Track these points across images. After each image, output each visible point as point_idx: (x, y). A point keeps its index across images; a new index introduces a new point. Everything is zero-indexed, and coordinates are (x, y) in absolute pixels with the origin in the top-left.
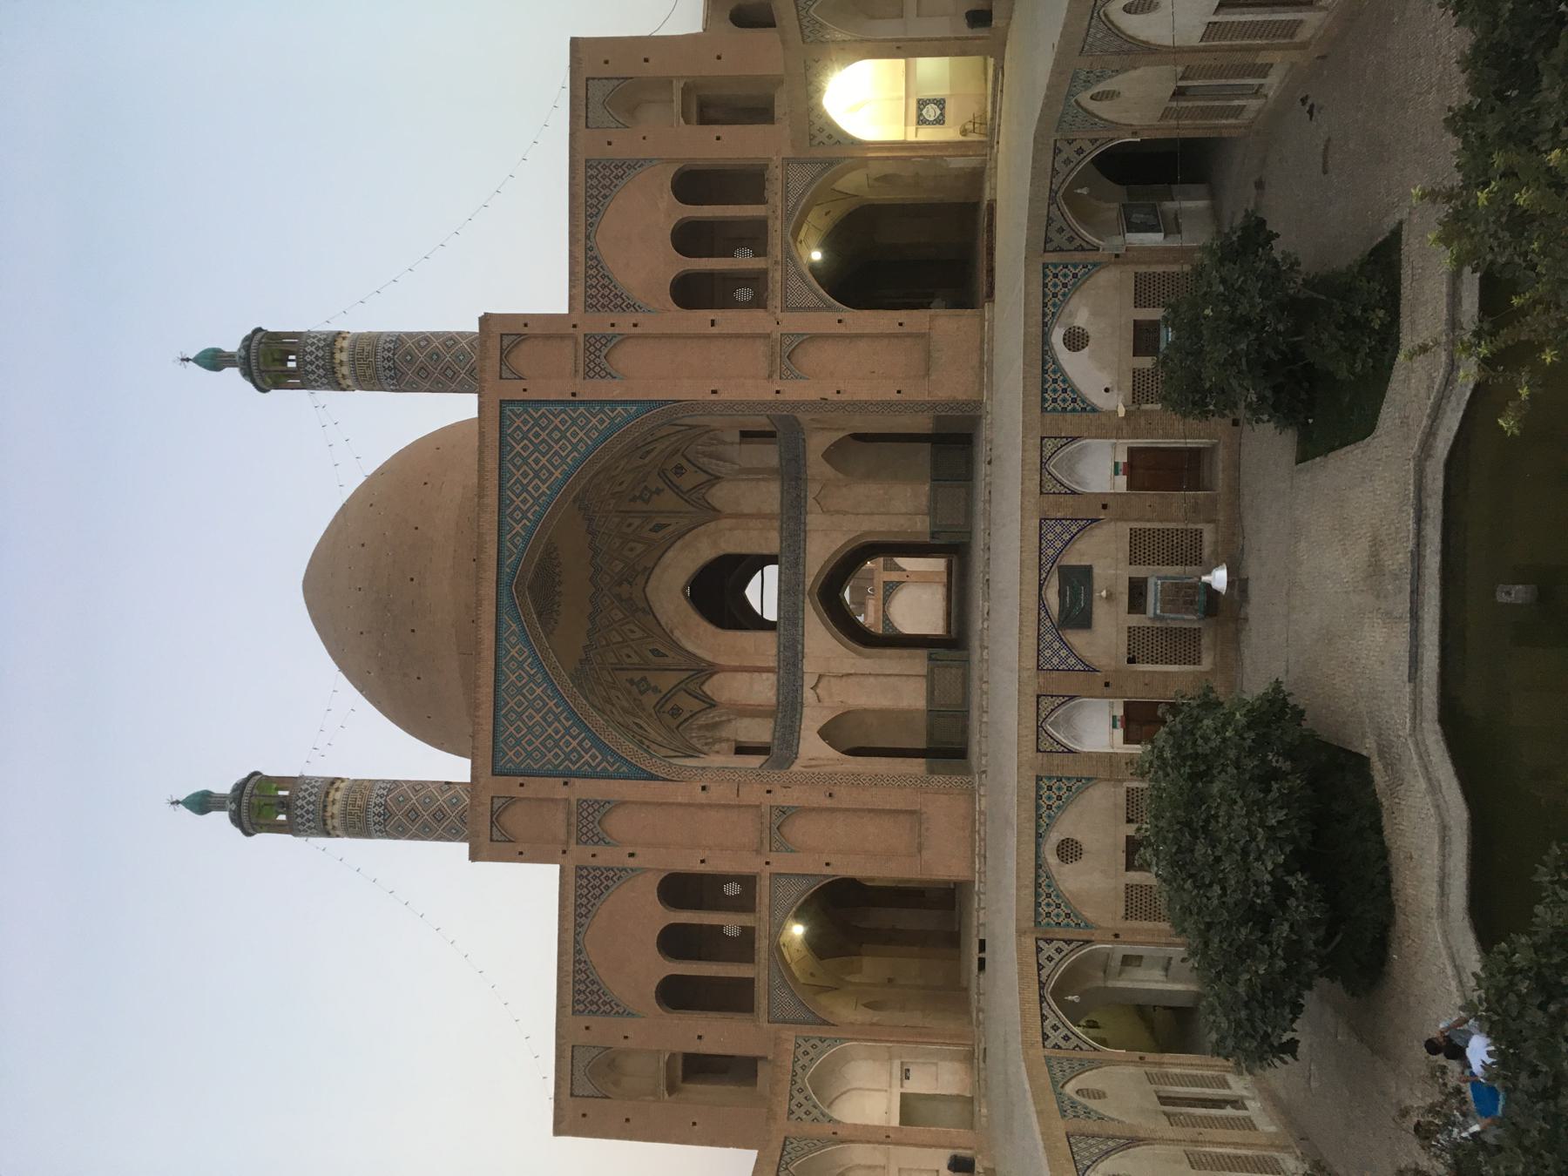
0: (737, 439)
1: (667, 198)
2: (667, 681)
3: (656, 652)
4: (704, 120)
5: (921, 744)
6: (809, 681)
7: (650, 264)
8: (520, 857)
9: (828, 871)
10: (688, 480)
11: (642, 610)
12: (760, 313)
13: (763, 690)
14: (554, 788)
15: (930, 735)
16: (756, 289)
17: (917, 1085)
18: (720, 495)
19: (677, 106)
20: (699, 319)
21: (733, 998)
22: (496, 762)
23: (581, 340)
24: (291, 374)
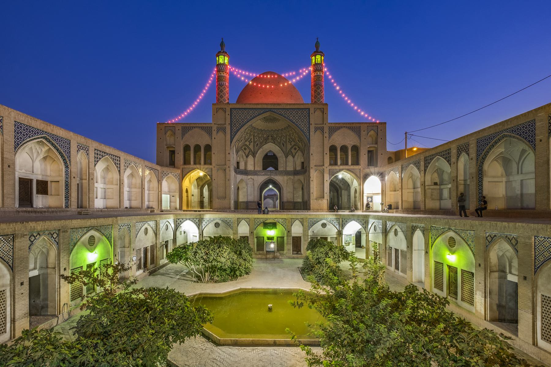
0: (302, 160)
1: (352, 143)
2: (251, 147)
3: (257, 144)
4: (369, 152)
6: (252, 177)
10: (293, 150)
11: (266, 141)
13: (250, 167)
14: (228, 121)
16: (334, 162)
18: (290, 158)
19: (371, 146)
20: (327, 150)
21: (186, 162)
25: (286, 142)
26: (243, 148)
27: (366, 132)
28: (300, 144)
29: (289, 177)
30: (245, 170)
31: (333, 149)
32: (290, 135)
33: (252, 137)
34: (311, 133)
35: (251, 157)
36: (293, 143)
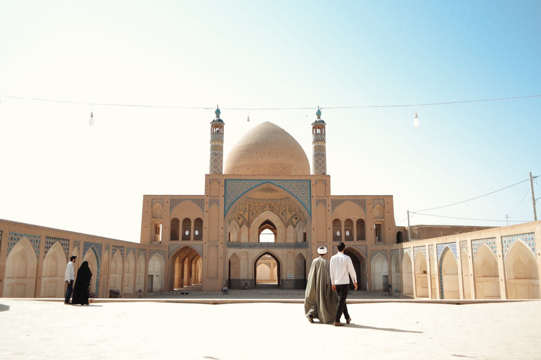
2: (246, 216)
3: (253, 214)
5: (232, 278)
6: (246, 250)
7: (343, 213)
8: (206, 186)
9: (204, 257)
10: (294, 220)
12: (332, 239)
13: (244, 239)
15: (234, 280)
17: (155, 278)
18: (290, 227)
20: (330, 225)
21: (174, 236)
22: (227, 181)
23: (324, 198)
24: (316, 131)
25: (285, 211)
26: (236, 218)
27: (371, 205)
28: (302, 215)
29: (289, 250)
30: (238, 242)
31: (336, 222)
32: (290, 205)
33: (247, 206)
34: (312, 206)
35: (245, 227)
36: (293, 213)
